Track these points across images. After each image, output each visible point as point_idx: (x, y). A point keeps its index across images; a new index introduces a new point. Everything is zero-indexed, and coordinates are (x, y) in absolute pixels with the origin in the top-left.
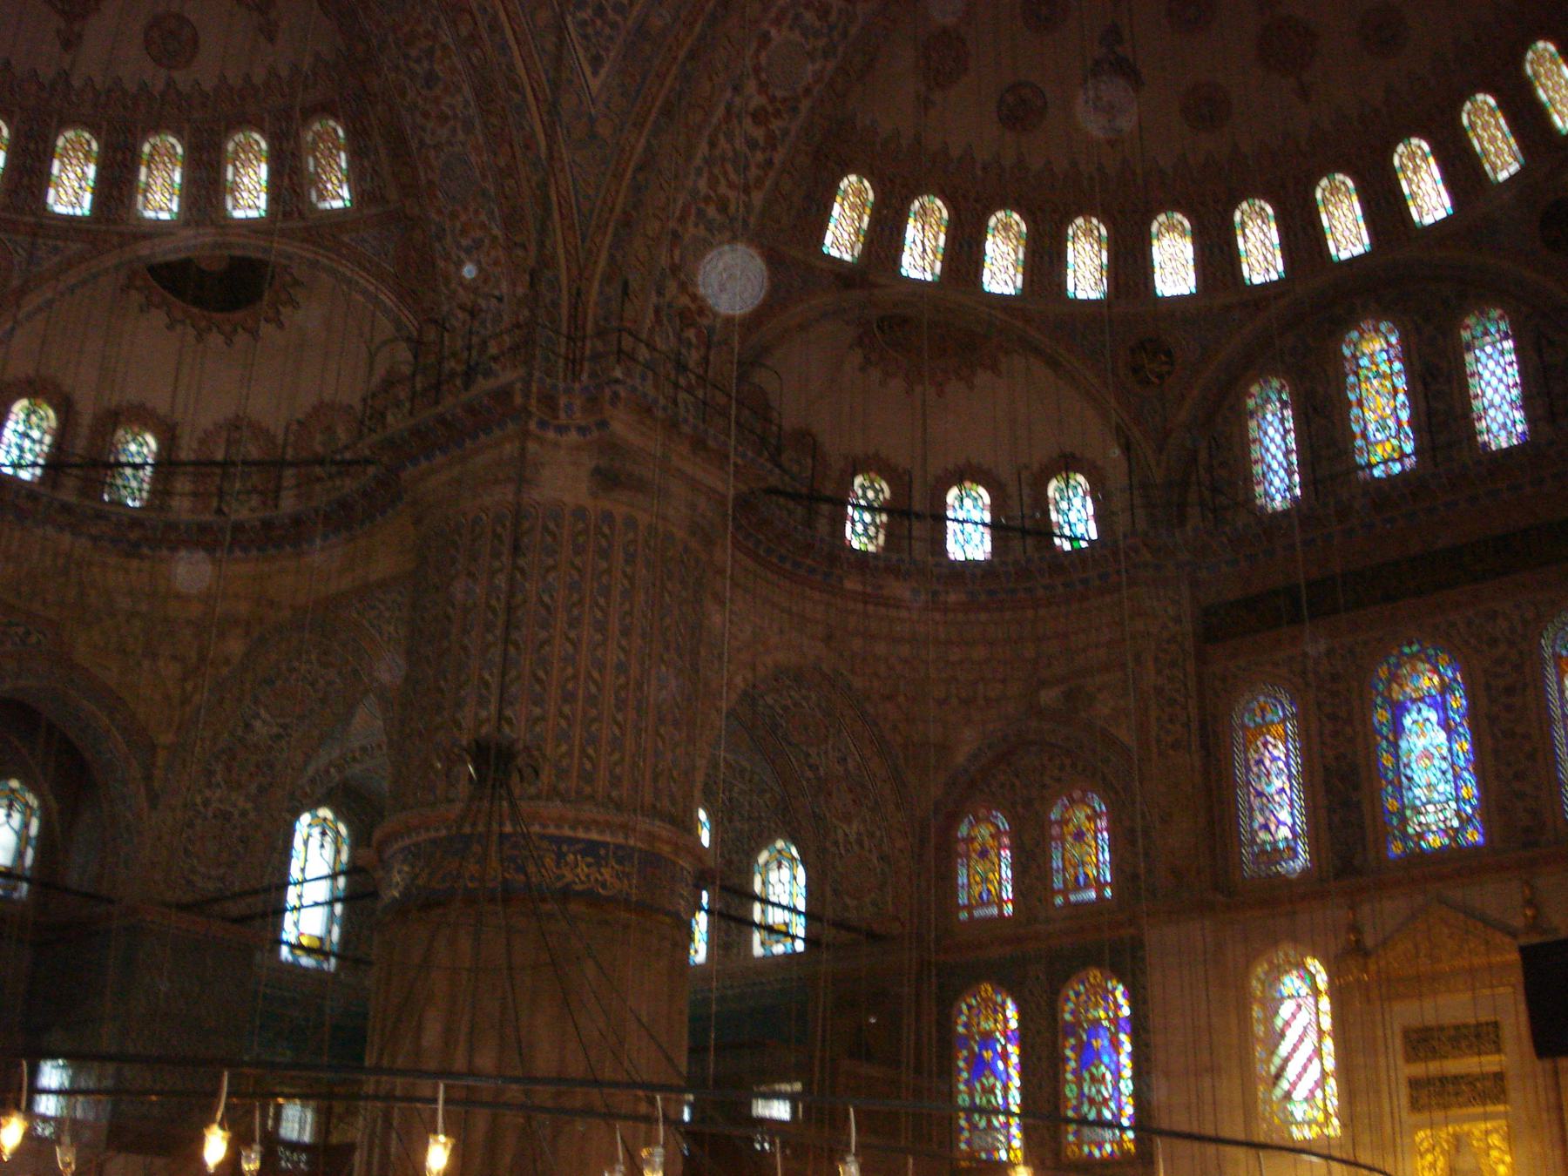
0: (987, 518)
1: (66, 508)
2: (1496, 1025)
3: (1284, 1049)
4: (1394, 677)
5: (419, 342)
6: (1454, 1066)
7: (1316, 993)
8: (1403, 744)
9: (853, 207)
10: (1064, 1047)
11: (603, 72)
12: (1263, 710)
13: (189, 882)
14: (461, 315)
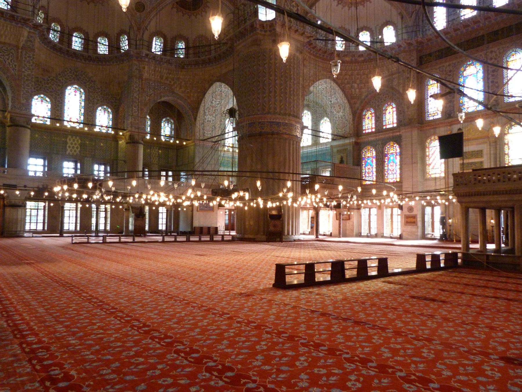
4: (465, 70)
14: (243, 6)
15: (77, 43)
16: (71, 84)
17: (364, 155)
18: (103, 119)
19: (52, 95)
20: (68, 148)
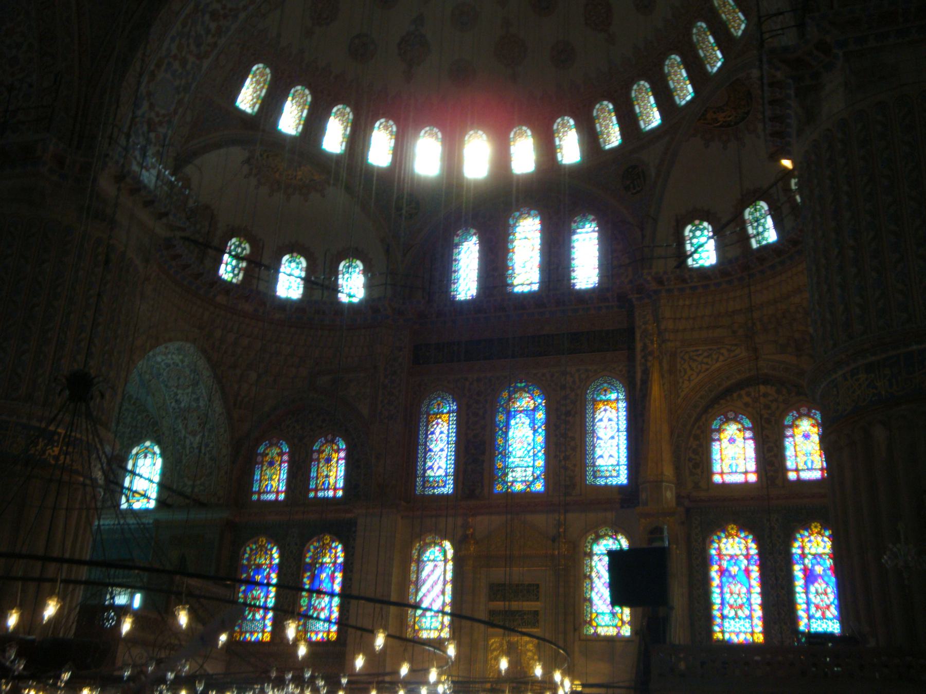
0: (303, 274)
2: (538, 586)
3: (424, 590)
6: (515, 605)
7: (446, 561)
8: (510, 434)
9: (258, 82)
10: (303, 577)
12: (439, 405)
17: (249, 559)
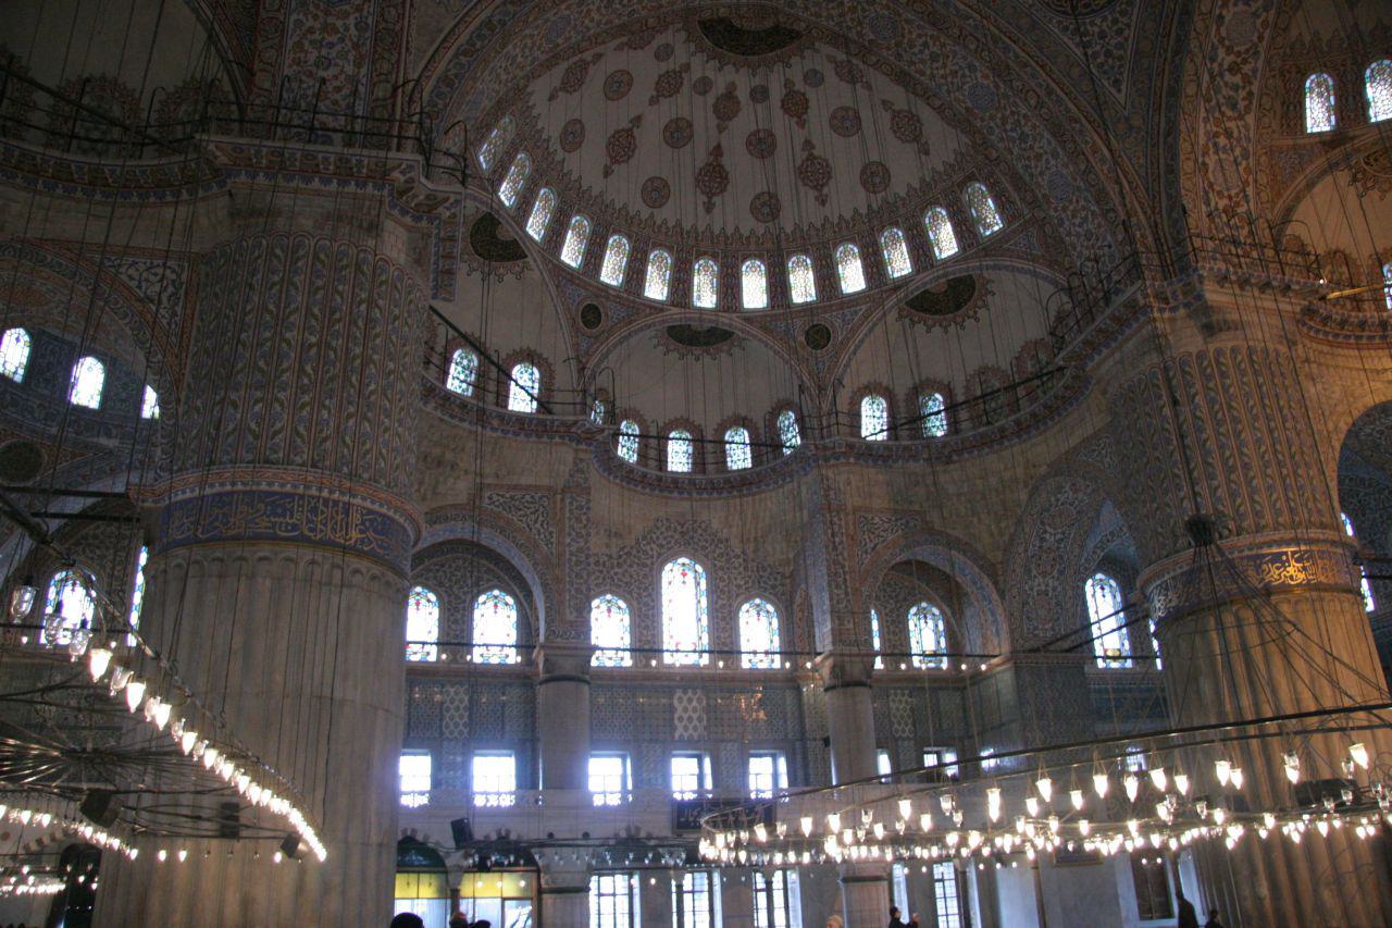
1: (906, 448)
5: (1070, 289)
9: (1320, 95)
11: (1123, 87)
13: (1036, 635)
14: (1090, 264)
15: (679, 456)
16: (672, 557)
18: (759, 634)
19: (630, 593)
20: (676, 722)
